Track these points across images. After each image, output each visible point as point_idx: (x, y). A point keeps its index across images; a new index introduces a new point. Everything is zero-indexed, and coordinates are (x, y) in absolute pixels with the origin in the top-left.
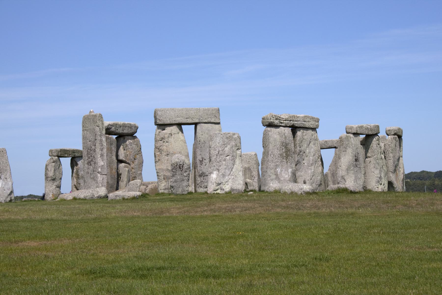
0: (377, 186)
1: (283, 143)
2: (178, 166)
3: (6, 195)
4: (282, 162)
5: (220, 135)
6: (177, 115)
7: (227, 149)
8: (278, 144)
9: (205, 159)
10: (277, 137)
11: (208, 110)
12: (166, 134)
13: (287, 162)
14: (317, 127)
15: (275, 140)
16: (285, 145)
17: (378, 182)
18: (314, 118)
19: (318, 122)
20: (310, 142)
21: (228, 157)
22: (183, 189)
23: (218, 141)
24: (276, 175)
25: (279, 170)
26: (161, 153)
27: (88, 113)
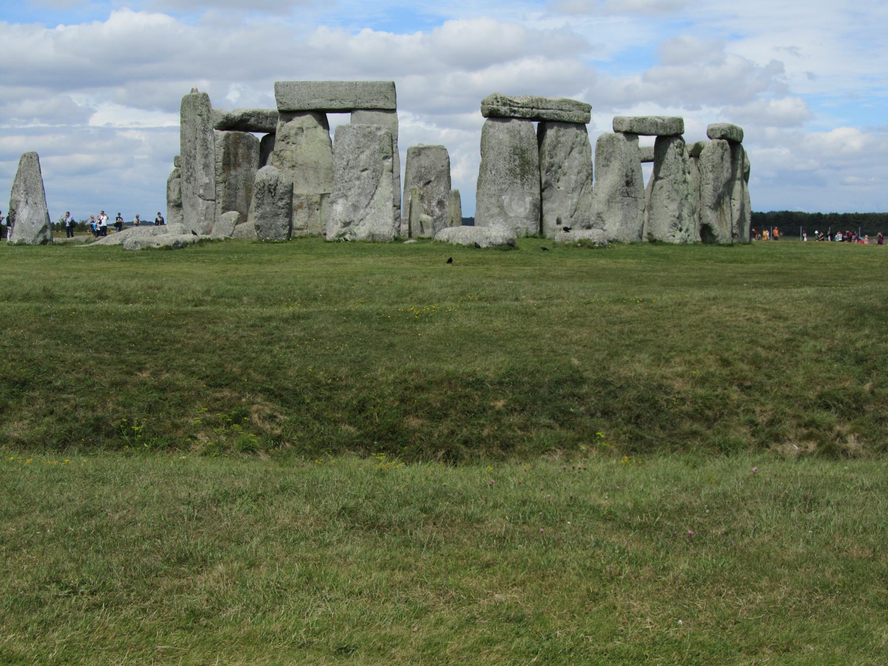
1: (515, 148)
2: (266, 188)
3: (36, 232)
4: (512, 183)
5: (351, 129)
7: (363, 157)
12: (293, 128)
13: (523, 184)
14: (587, 120)
15: (500, 143)
16: (519, 153)
17: (675, 225)
18: (581, 104)
19: (589, 112)
20: (572, 149)
21: (365, 173)
22: (277, 231)
23: (348, 142)
24: (501, 207)
25: (506, 198)
27: (188, 93)
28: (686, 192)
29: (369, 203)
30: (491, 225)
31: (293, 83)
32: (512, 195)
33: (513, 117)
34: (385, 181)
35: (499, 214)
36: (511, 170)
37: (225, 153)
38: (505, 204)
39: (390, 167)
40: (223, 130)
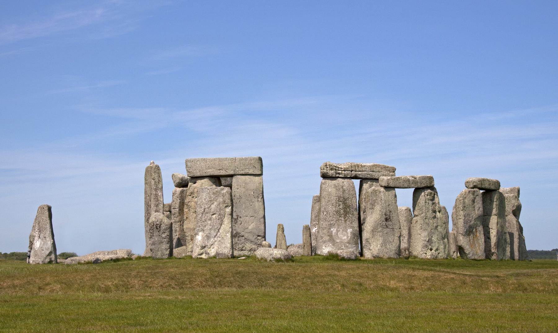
0: (425, 252)
1: (339, 197)
4: (338, 220)
5: (207, 190)
6: (207, 166)
7: (213, 206)
8: (334, 199)
9: (240, 217)
10: (332, 190)
11: (246, 159)
13: (346, 221)
15: (330, 194)
17: (426, 246)
18: (388, 167)
19: (394, 172)
21: (214, 216)
24: (330, 235)
25: (334, 230)
26: (189, 210)
28: (435, 225)
29: (217, 235)
30: (324, 247)
31: (195, 159)
32: (338, 228)
33: (338, 177)
34: (227, 221)
35: (329, 240)
36: (337, 212)
37: (180, 202)
38: (333, 234)
39: (230, 212)
40: (180, 187)
